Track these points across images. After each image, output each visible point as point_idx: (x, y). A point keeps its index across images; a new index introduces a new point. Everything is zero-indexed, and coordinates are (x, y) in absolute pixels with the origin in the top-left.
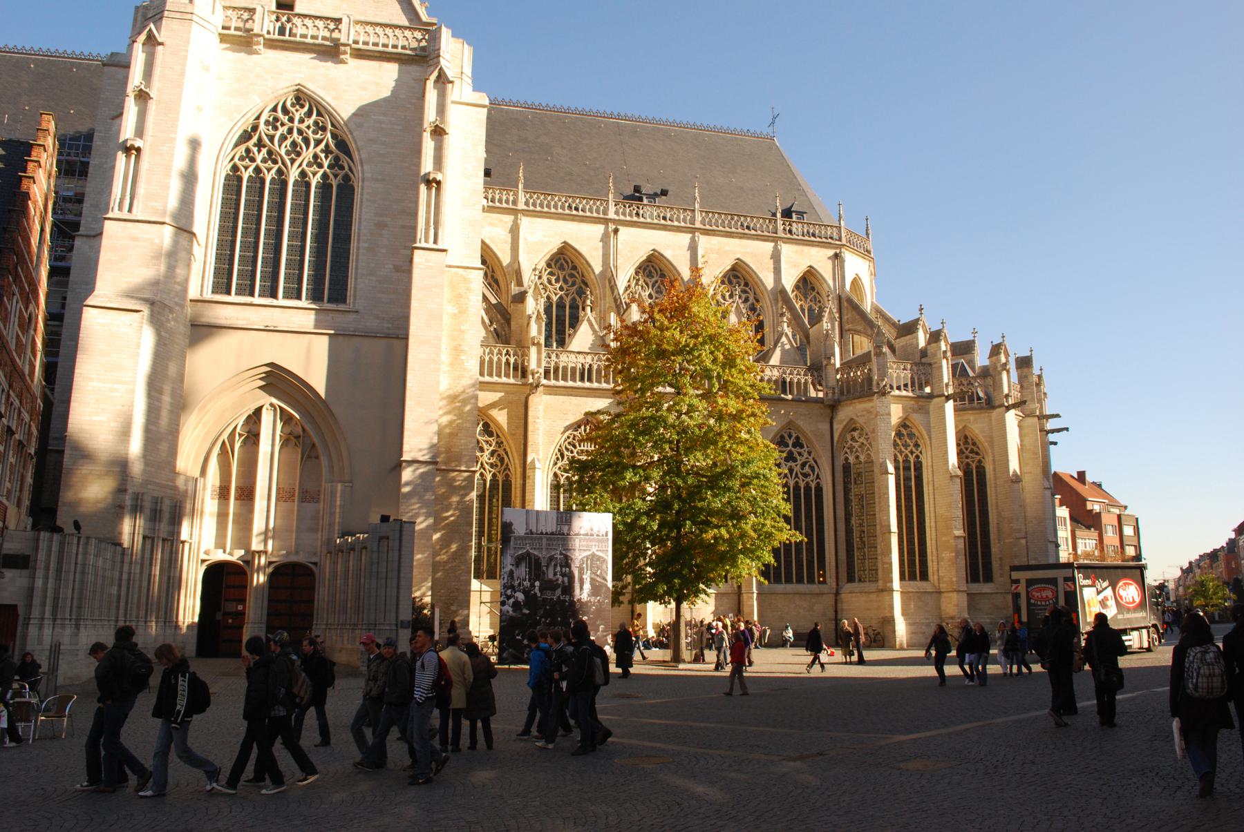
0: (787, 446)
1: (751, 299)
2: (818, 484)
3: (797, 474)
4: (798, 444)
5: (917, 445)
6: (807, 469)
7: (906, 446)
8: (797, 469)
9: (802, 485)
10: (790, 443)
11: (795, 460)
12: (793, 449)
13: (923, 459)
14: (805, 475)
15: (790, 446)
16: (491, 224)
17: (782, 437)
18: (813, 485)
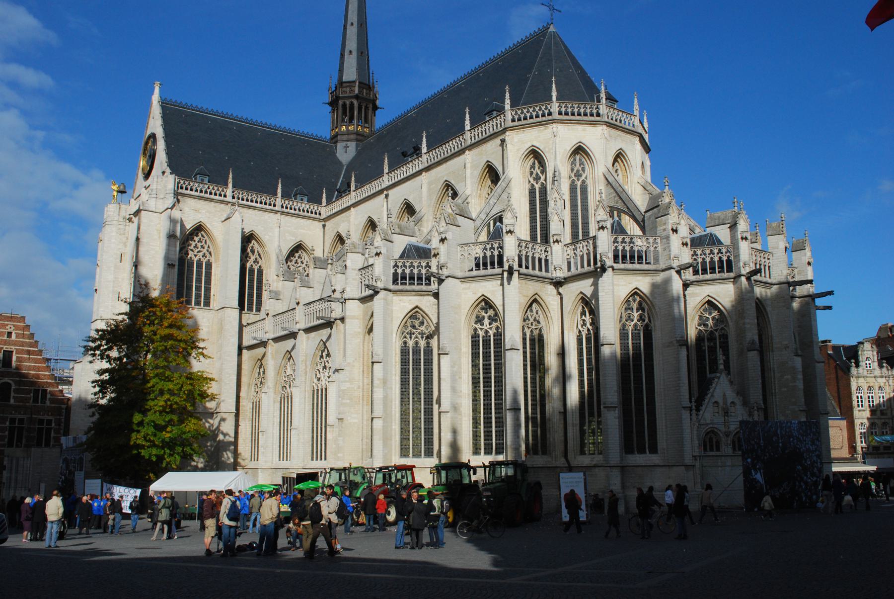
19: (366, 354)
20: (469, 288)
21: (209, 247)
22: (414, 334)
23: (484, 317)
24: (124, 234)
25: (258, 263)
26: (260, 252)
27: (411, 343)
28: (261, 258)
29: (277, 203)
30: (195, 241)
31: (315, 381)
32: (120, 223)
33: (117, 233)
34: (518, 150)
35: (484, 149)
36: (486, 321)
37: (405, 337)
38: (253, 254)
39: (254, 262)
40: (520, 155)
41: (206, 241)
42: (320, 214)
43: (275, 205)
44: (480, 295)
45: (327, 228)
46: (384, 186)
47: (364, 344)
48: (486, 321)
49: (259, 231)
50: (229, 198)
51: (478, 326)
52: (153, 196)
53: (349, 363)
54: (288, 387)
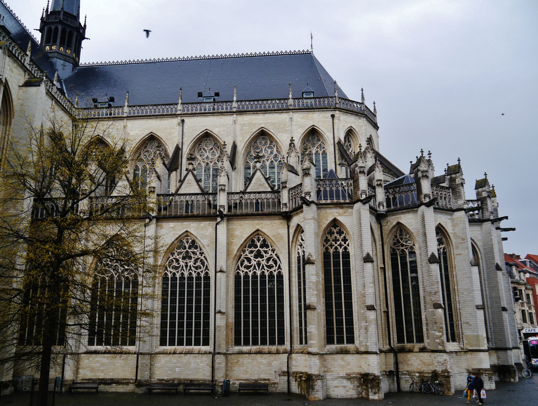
0: (256, 246)
1: (275, 152)
2: (280, 272)
3: (263, 266)
4: (265, 245)
5: (345, 240)
6: (271, 262)
7: (336, 240)
8: (264, 263)
9: (267, 274)
10: (259, 244)
11: (262, 257)
12: (261, 249)
13: (351, 249)
14: (270, 267)
15: (259, 247)
17: (253, 241)
18: (275, 274)
35: (309, 116)
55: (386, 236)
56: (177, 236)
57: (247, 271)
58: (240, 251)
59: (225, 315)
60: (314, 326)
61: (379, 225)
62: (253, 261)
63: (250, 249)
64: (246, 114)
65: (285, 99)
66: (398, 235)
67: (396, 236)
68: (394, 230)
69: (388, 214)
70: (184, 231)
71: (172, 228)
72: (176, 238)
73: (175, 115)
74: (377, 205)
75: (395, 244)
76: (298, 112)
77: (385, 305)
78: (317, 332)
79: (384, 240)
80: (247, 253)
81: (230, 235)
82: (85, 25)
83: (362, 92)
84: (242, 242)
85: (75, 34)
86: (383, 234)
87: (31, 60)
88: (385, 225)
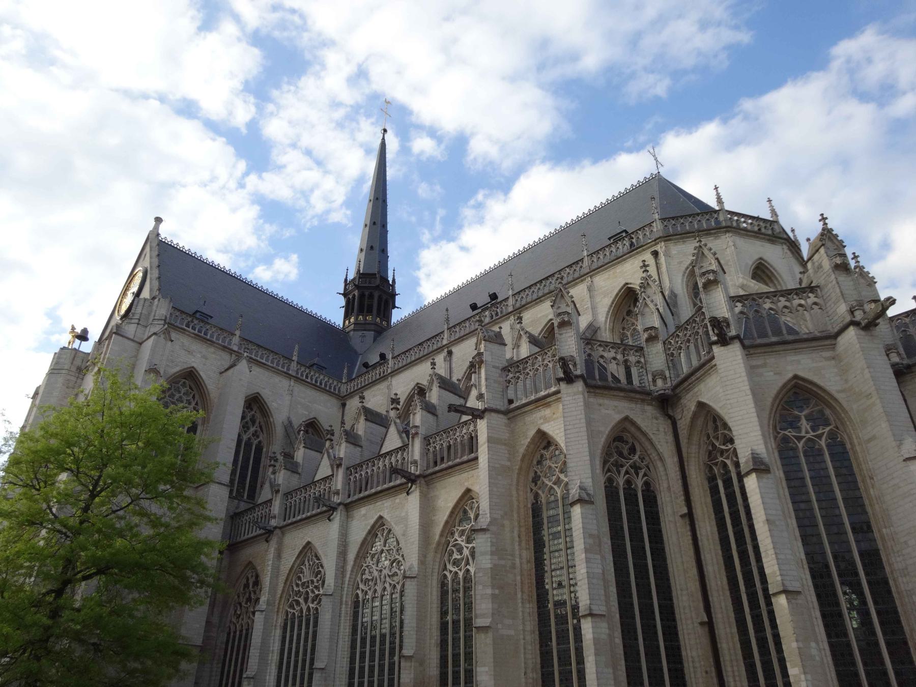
16: (374, 396)
19: (522, 506)
20: (764, 365)
21: (197, 404)
22: (622, 466)
23: (798, 418)
24: (73, 388)
25: (258, 437)
26: (262, 423)
27: (621, 481)
28: (262, 431)
29: (292, 368)
30: (180, 392)
31: (361, 586)
32: (71, 373)
33: (63, 385)
34: (680, 263)
36: (805, 424)
37: (609, 470)
38: (253, 425)
39: (253, 435)
40: (684, 269)
41: (194, 395)
42: (339, 391)
43: (288, 369)
44: (790, 375)
45: (347, 407)
46: (445, 342)
47: (517, 490)
48: (805, 424)
49: (267, 395)
50: (235, 348)
51: (789, 433)
52: (133, 321)
53: (495, 519)
54: (301, 600)
55: (685, 441)
56: (369, 528)
57: (456, 569)
58: (445, 535)
59: (413, 660)
60: (486, 669)
61: (669, 421)
62: (465, 549)
63: (460, 528)
64: (527, 308)
65: (577, 263)
66: (711, 432)
67: (708, 437)
68: (700, 422)
69: (678, 391)
70: (376, 517)
71: (364, 515)
72: (367, 531)
73: (440, 350)
74: (650, 379)
75: (710, 453)
76: (599, 272)
77: (701, 605)
78: (492, 682)
79: (684, 450)
80: (456, 536)
81: (427, 509)
82: (394, 280)
83: (717, 191)
84: (445, 518)
85: (376, 295)
86: (681, 438)
87: (243, 339)
88: (679, 417)
